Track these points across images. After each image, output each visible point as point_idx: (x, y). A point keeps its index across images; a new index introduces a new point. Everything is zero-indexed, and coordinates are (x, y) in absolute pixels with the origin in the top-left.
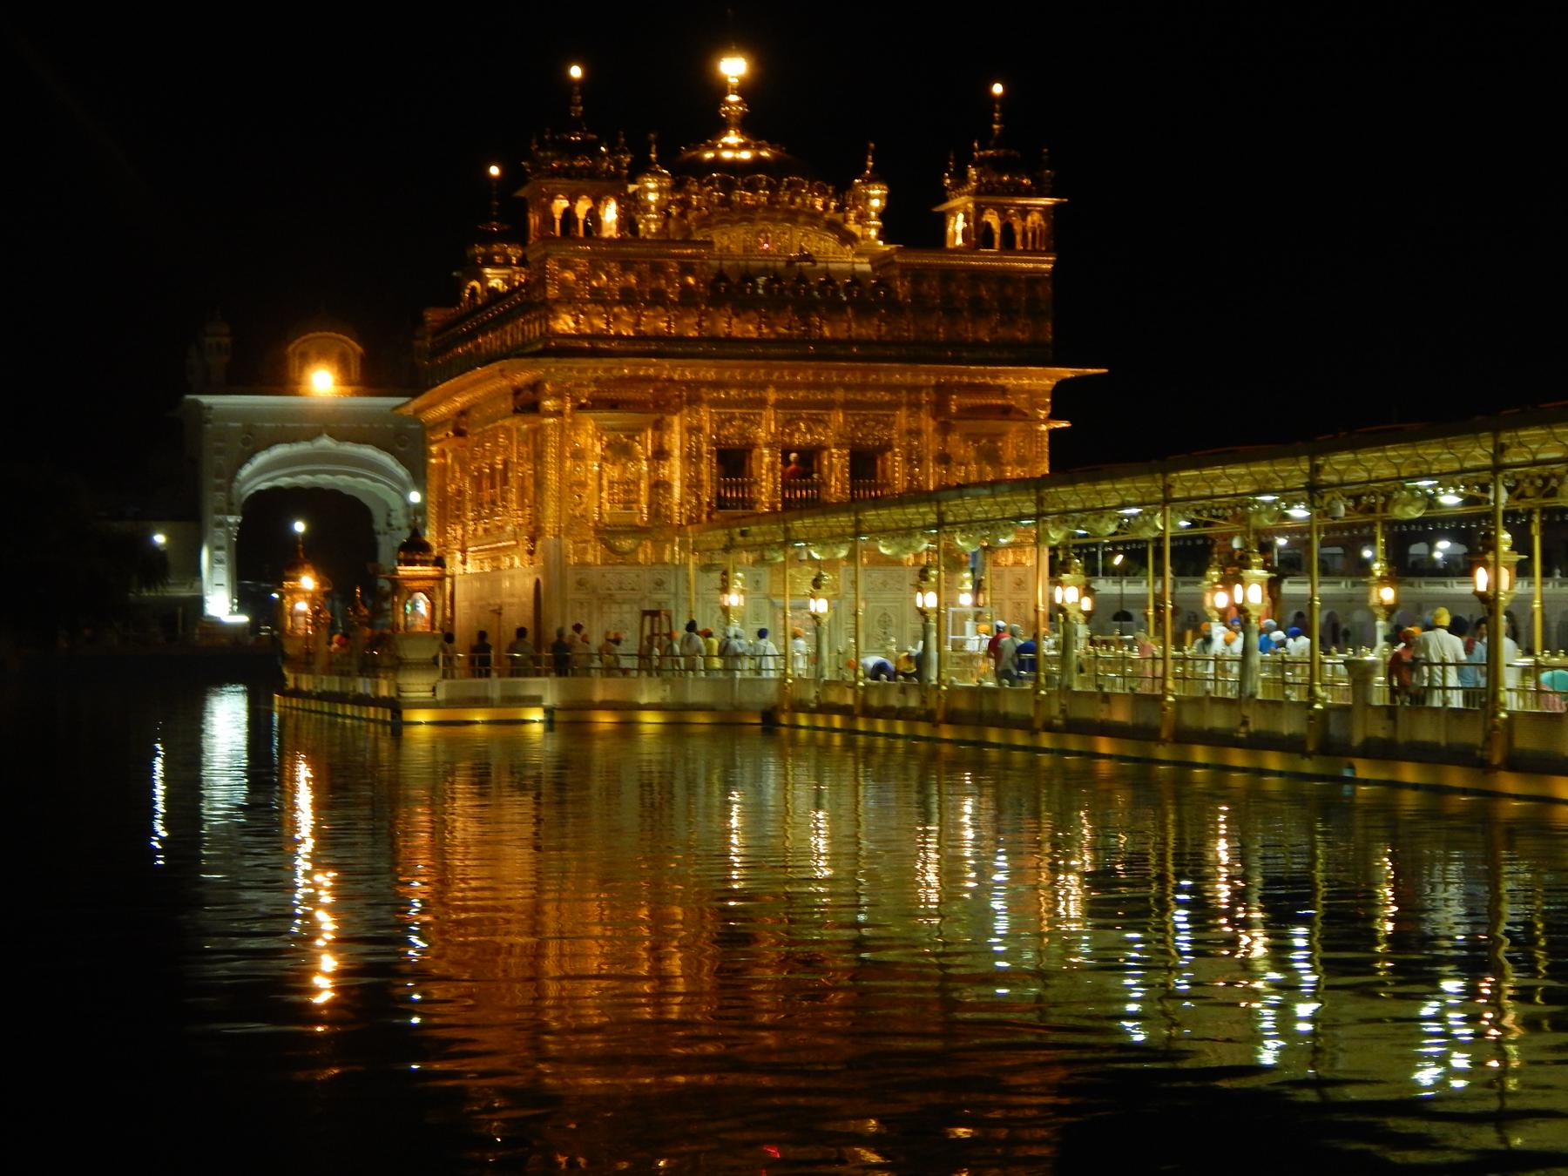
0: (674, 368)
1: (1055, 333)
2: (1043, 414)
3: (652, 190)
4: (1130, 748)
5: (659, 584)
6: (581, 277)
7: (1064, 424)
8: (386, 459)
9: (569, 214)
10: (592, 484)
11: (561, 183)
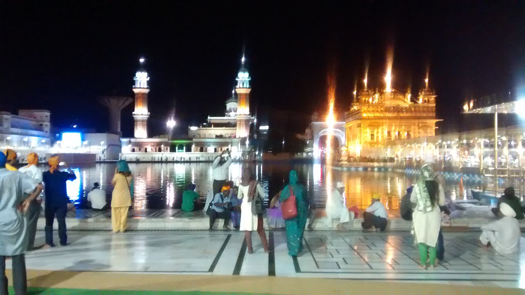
3: (377, 96)
8: (340, 131)
9: (365, 100)
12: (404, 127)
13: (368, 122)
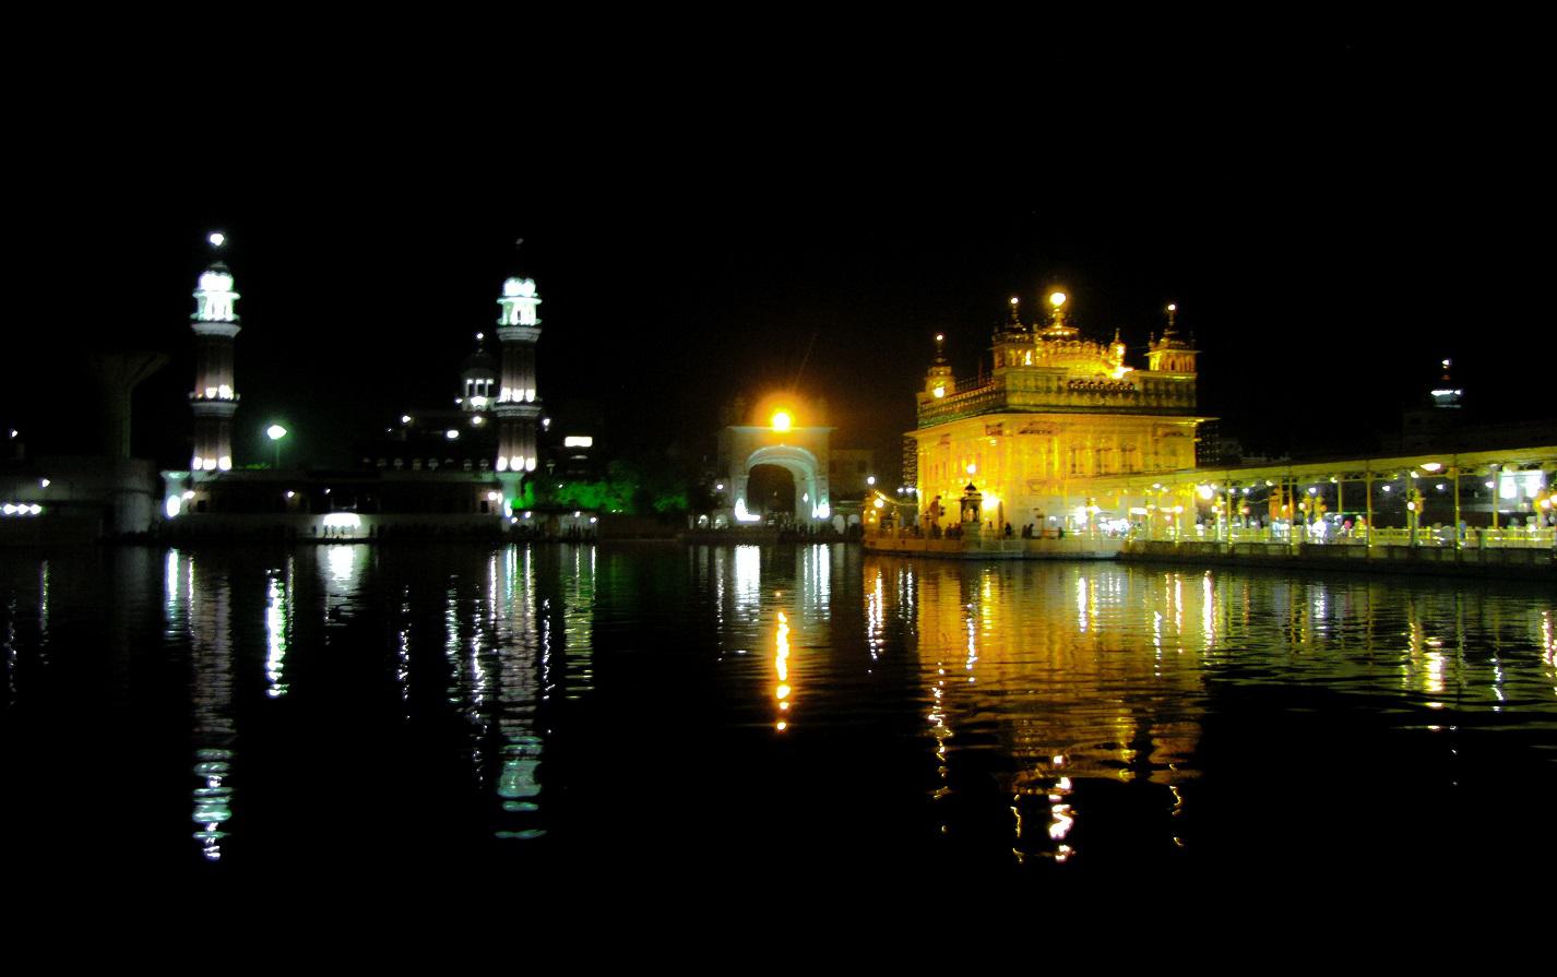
8: (807, 453)
12: (1115, 437)
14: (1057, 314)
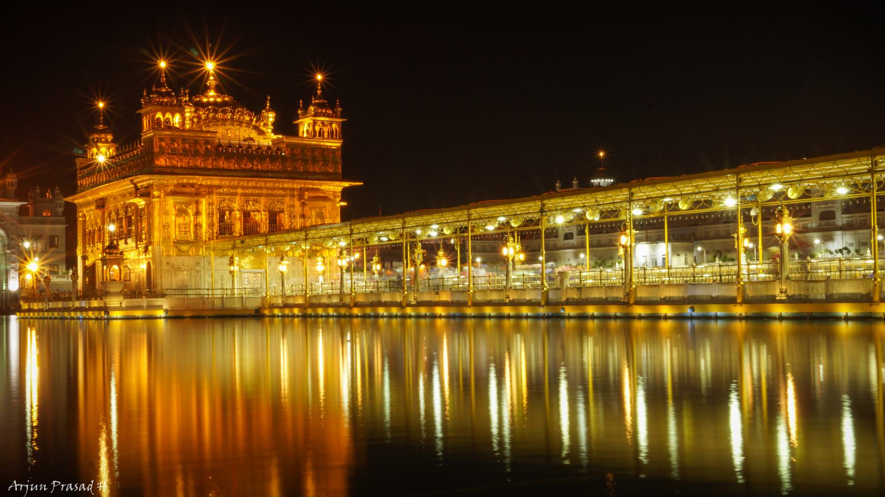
0: (203, 180)
1: (342, 169)
2: (338, 199)
4: (452, 311)
5: (198, 263)
6: (167, 144)
7: (345, 204)
10: (173, 226)
11: (160, 107)
13: (172, 181)
14: (212, 81)
